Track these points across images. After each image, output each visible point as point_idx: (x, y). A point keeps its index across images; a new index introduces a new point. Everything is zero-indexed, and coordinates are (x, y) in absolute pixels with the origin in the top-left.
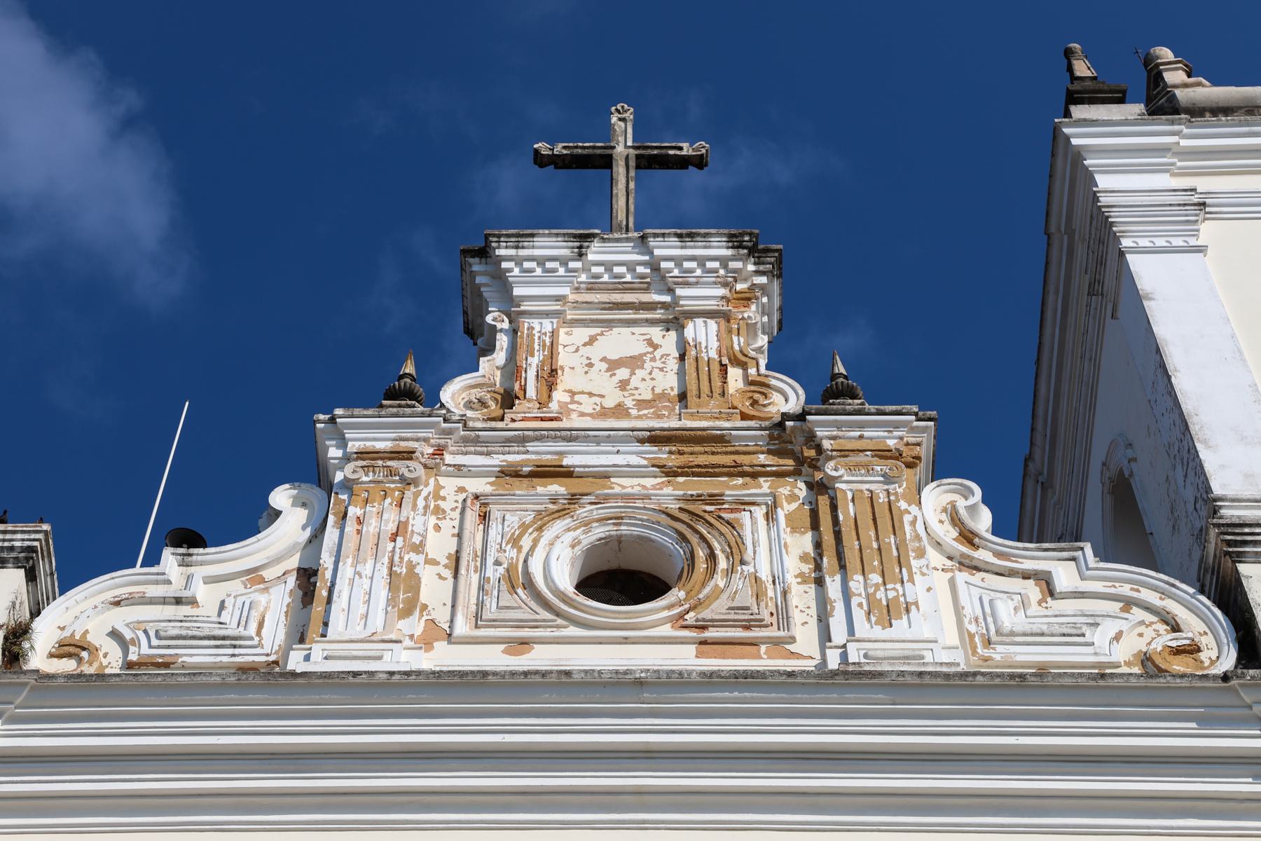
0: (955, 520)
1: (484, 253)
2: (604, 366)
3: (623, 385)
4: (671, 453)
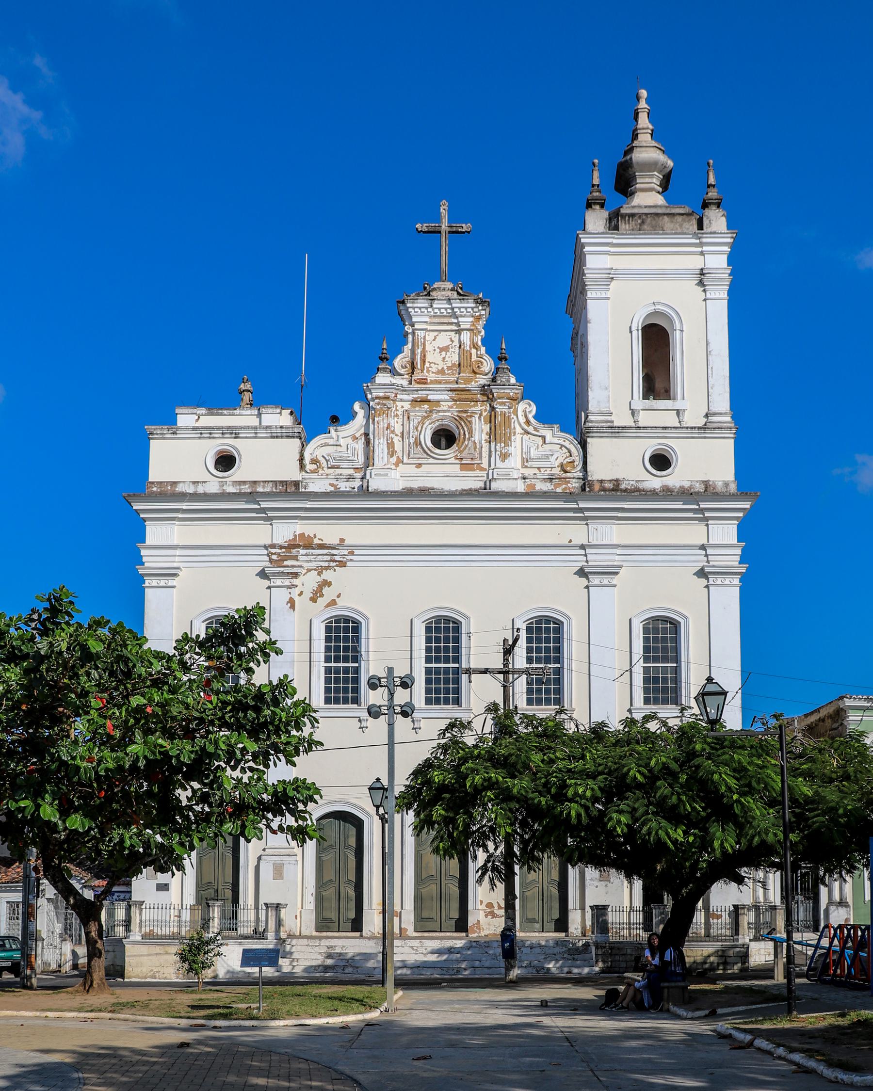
0: (526, 416)
1: (403, 302)
2: (438, 350)
3: (444, 358)
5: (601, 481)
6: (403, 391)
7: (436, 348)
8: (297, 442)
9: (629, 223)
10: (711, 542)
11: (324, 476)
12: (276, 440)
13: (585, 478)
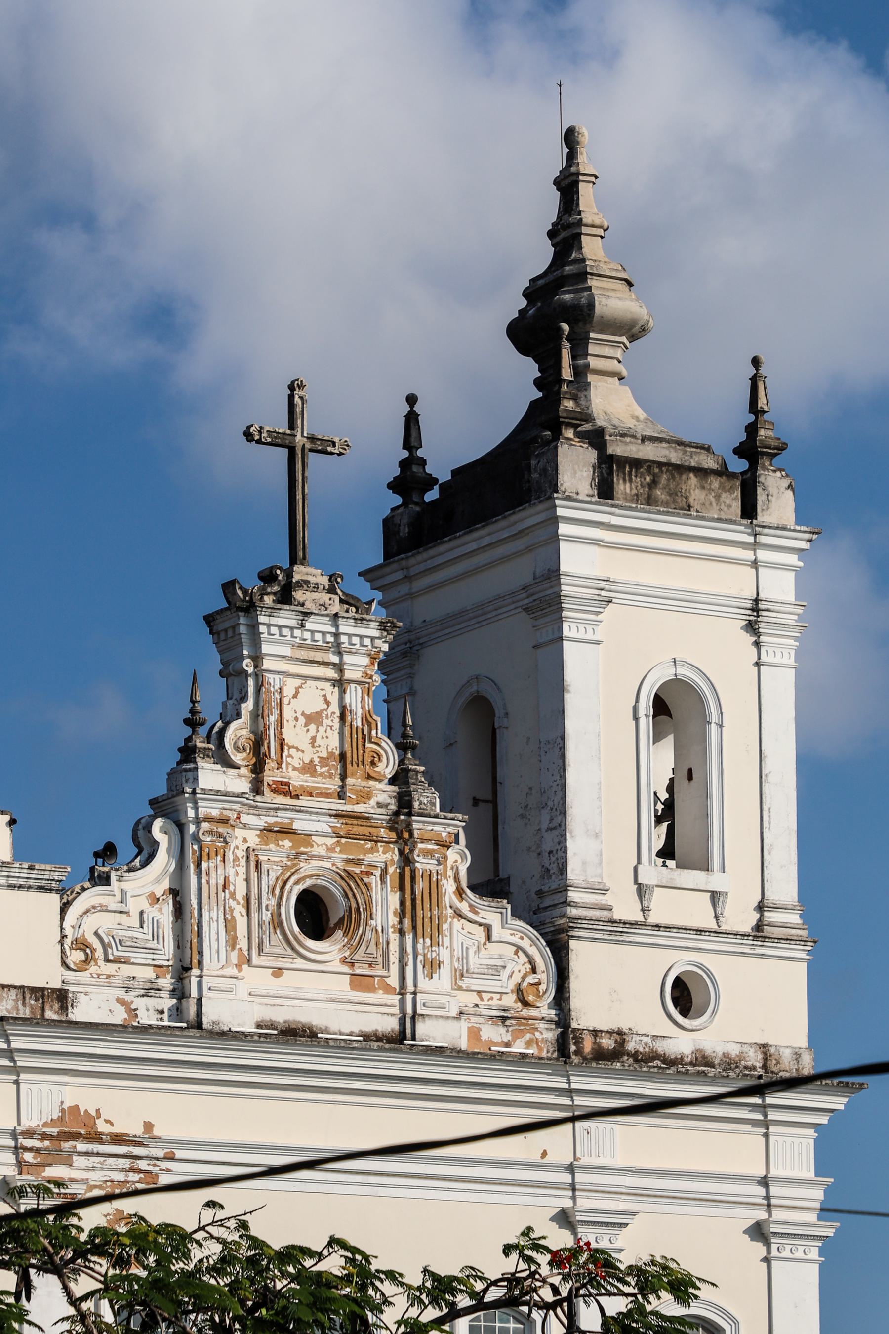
2: (302, 720)
3: (314, 739)
4: (342, 823)
5: (595, 1033)
6: (251, 806)
7: (299, 715)
8: (54, 901)
9: (631, 481)
10: (773, 1172)
11: (103, 979)
12: (16, 893)
13: (563, 1021)
